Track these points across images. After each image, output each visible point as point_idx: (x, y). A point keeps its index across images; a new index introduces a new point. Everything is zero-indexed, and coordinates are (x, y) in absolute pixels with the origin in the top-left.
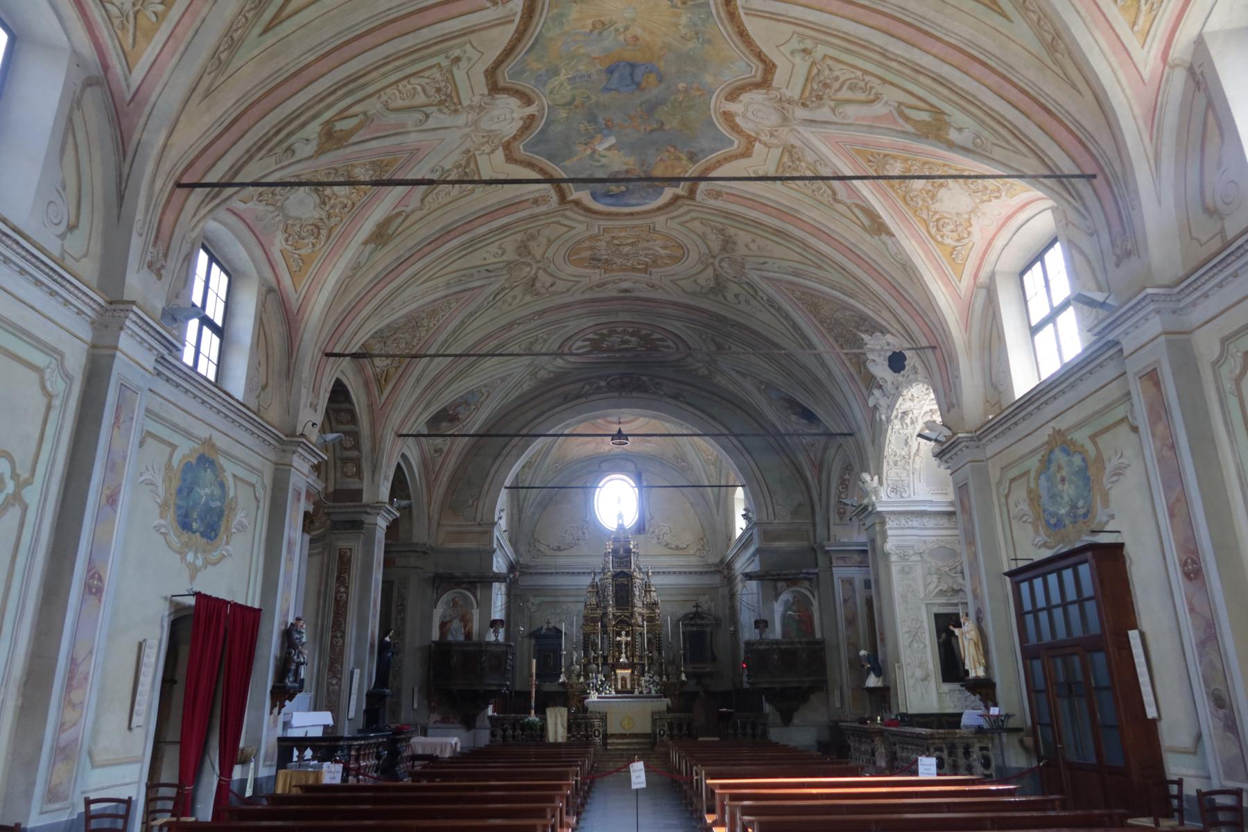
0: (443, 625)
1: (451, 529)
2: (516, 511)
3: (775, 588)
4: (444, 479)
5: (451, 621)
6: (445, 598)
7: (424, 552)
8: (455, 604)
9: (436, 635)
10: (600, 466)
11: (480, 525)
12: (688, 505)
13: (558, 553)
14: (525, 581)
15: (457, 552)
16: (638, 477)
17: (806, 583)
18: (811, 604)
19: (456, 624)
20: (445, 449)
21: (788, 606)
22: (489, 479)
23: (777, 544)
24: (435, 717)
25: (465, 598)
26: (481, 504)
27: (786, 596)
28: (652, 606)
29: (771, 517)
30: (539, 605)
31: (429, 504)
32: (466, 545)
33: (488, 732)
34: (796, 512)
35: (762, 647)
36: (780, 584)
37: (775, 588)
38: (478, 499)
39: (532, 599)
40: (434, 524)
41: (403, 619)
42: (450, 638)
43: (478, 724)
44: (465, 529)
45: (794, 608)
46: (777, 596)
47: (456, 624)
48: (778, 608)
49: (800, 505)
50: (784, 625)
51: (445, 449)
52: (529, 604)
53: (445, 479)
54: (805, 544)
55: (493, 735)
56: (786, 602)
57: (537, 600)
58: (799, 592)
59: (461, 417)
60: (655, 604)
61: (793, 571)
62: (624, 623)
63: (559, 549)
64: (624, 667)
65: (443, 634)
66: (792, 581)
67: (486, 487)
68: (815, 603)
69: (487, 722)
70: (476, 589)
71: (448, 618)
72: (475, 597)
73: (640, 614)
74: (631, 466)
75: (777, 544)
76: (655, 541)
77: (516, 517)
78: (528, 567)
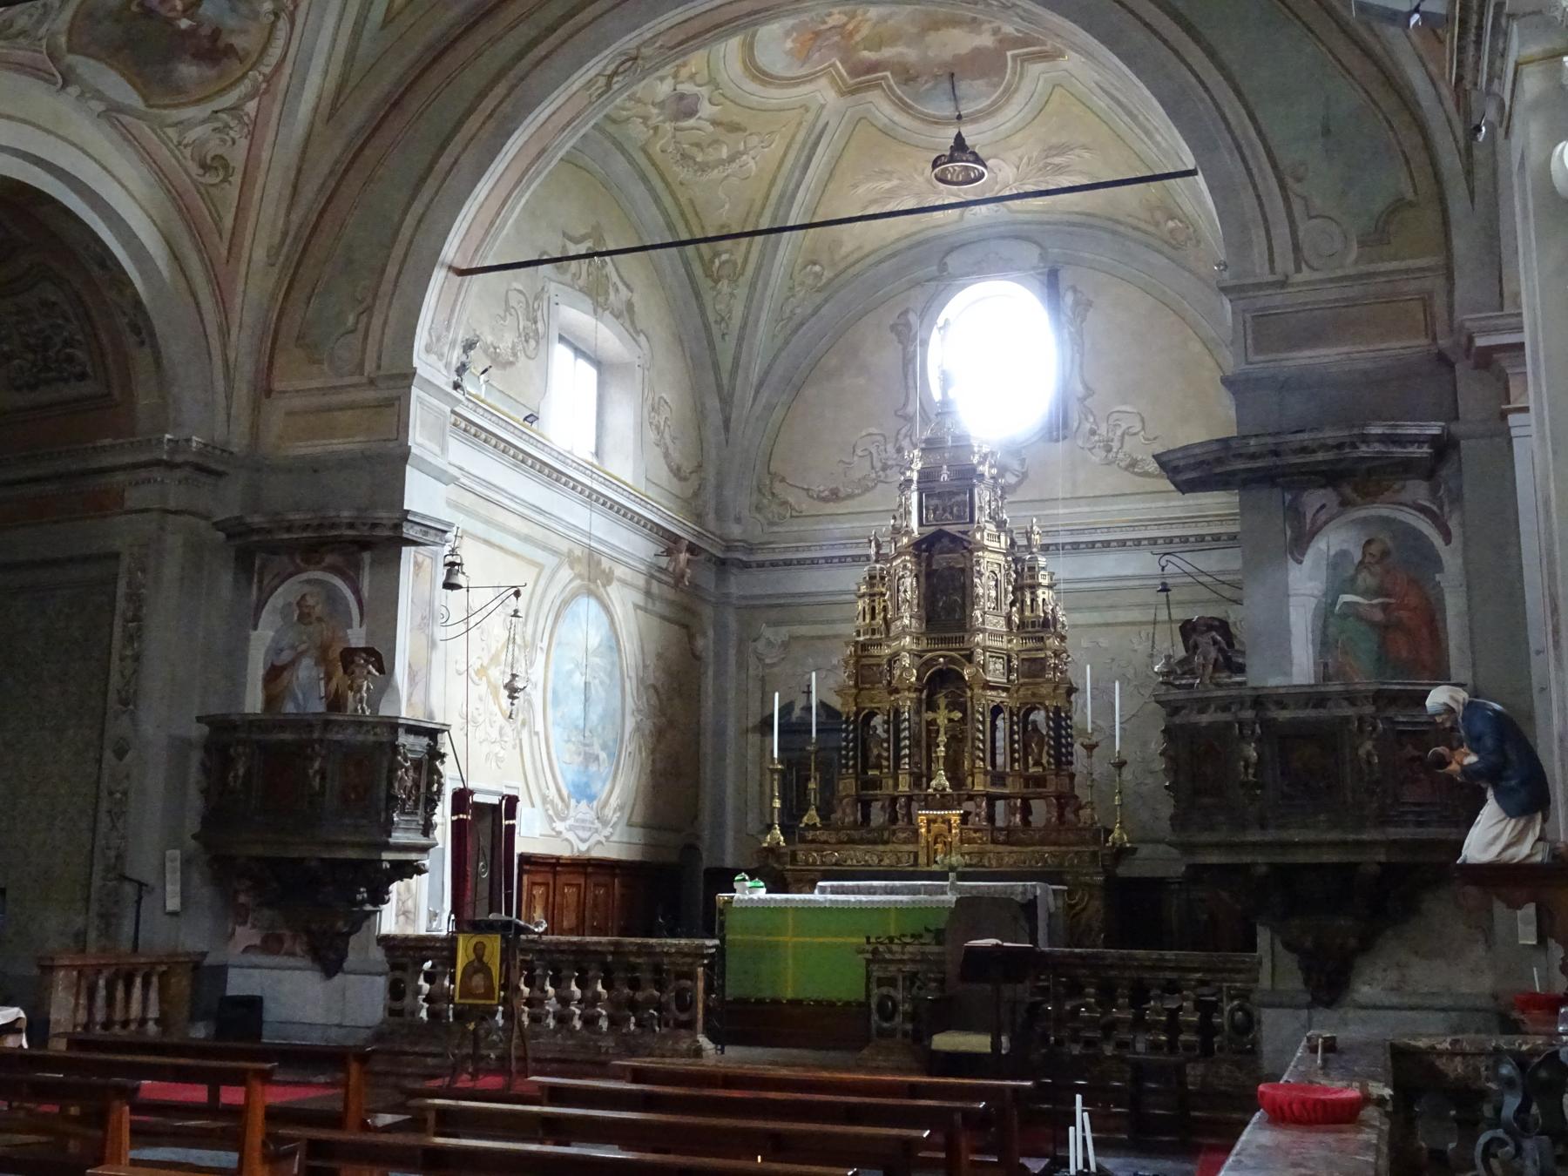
0: (274, 674)
1: (298, 403)
2: (713, 403)
3: (1294, 512)
4: (258, 248)
5: (293, 663)
6: (278, 600)
7: (206, 468)
8: (304, 617)
9: (254, 702)
10: (931, 268)
11: (372, 382)
12: (1197, 347)
13: (831, 508)
14: (739, 585)
15: (315, 467)
16: (1051, 282)
17: (1418, 490)
18: (1436, 563)
19: (306, 671)
20: (237, 157)
21: (1340, 576)
22: (398, 251)
23: (1304, 357)
24: (246, 935)
25: (333, 597)
26: (377, 322)
27: (1337, 541)
28: (1037, 628)
29: (1285, 263)
30: (785, 645)
31: (225, 332)
32: (339, 445)
33: (382, 982)
34: (1379, 235)
35: (1205, 719)
36: (1314, 499)
37: (1294, 512)
38: (369, 310)
39: (768, 633)
40: (243, 389)
41: (137, 658)
42: (290, 708)
43: (352, 959)
44: (335, 399)
45: (1366, 579)
46: (1299, 544)
47: (306, 671)
48: (1305, 584)
49: (1399, 205)
50: (1324, 644)
51: (237, 157)
52: (760, 645)
53: (260, 254)
54: (1406, 346)
55: (396, 991)
56: (1337, 562)
57: (784, 632)
58: (1386, 522)
59: (239, 42)
60: (1047, 624)
61: (1330, 434)
62: (943, 682)
63: (835, 496)
64: (944, 802)
65: (271, 701)
66: (1352, 477)
67: (391, 271)
68: (1451, 558)
69: (378, 954)
70: (358, 567)
71: (286, 656)
72: (357, 592)
73: (996, 653)
74: (1031, 253)
75: (1304, 357)
76: (1098, 456)
77: (715, 419)
78: (751, 549)
